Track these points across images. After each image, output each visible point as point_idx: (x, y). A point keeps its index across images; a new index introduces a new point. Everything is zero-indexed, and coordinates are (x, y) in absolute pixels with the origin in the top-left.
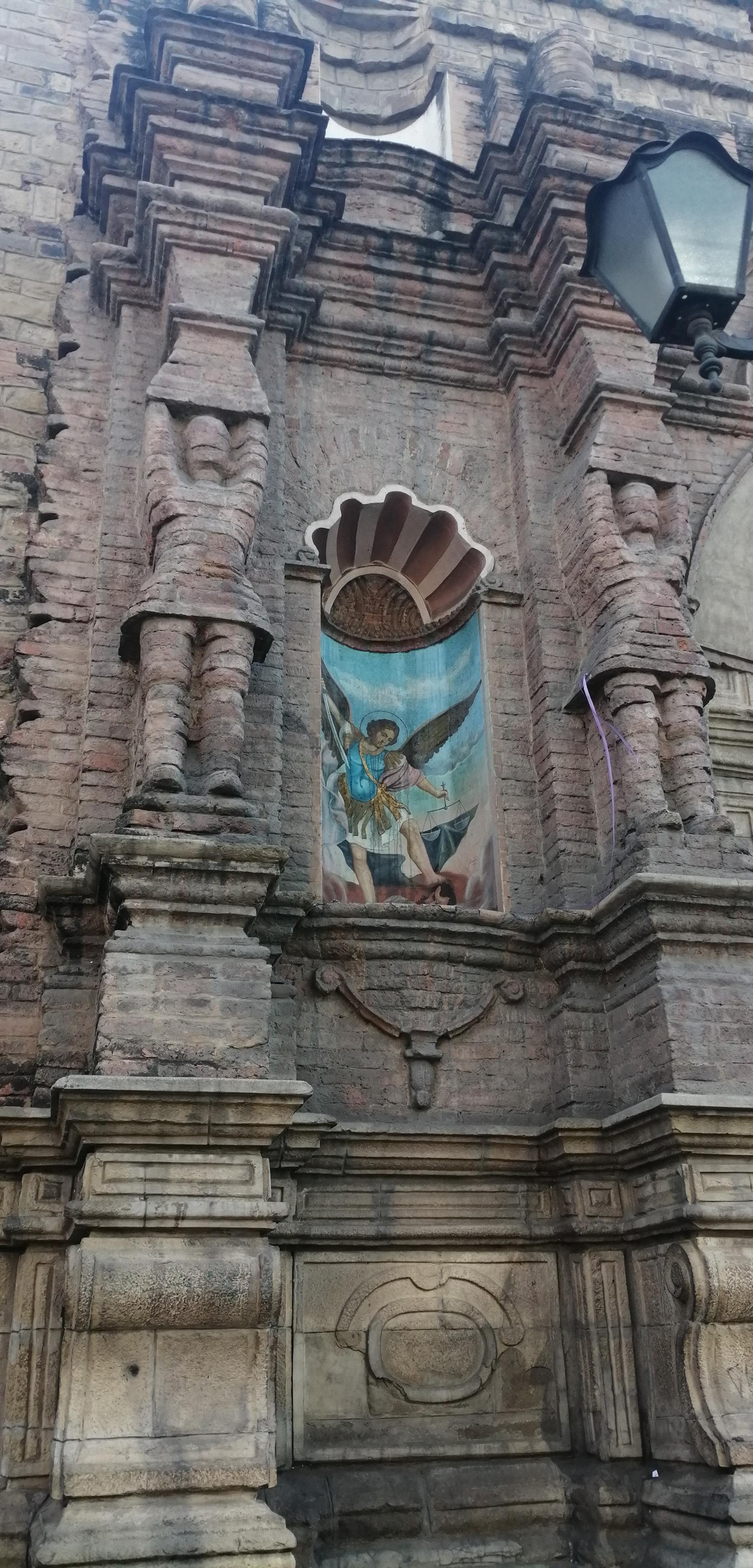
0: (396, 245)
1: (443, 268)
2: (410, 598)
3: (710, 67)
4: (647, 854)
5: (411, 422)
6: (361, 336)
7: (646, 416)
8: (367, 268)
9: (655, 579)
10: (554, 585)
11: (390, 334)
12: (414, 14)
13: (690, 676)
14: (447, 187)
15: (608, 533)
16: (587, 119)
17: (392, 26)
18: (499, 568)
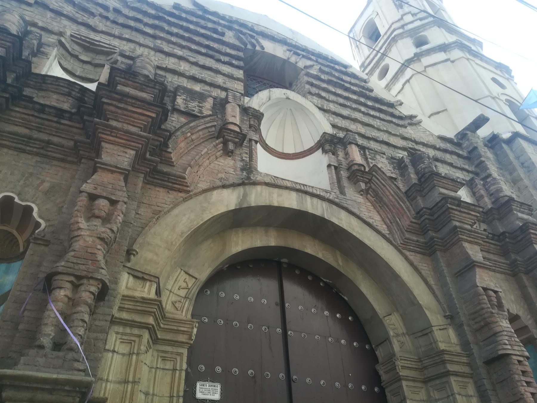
0: (46, 109)
1: (66, 120)
2: (18, 241)
3: (224, 83)
4: (20, 360)
5: (30, 171)
6: (17, 137)
7: (115, 175)
8: (33, 116)
9: (91, 236)
10: (62, 237)
11: (30, 138)
12: (116, 51)
13: (92, 278)
14: (85, 96)
15: (77, 216)
16: (133, 78)
17: (108, 54)
18: (46, 229)
